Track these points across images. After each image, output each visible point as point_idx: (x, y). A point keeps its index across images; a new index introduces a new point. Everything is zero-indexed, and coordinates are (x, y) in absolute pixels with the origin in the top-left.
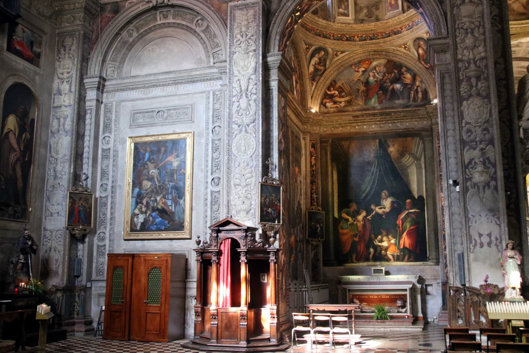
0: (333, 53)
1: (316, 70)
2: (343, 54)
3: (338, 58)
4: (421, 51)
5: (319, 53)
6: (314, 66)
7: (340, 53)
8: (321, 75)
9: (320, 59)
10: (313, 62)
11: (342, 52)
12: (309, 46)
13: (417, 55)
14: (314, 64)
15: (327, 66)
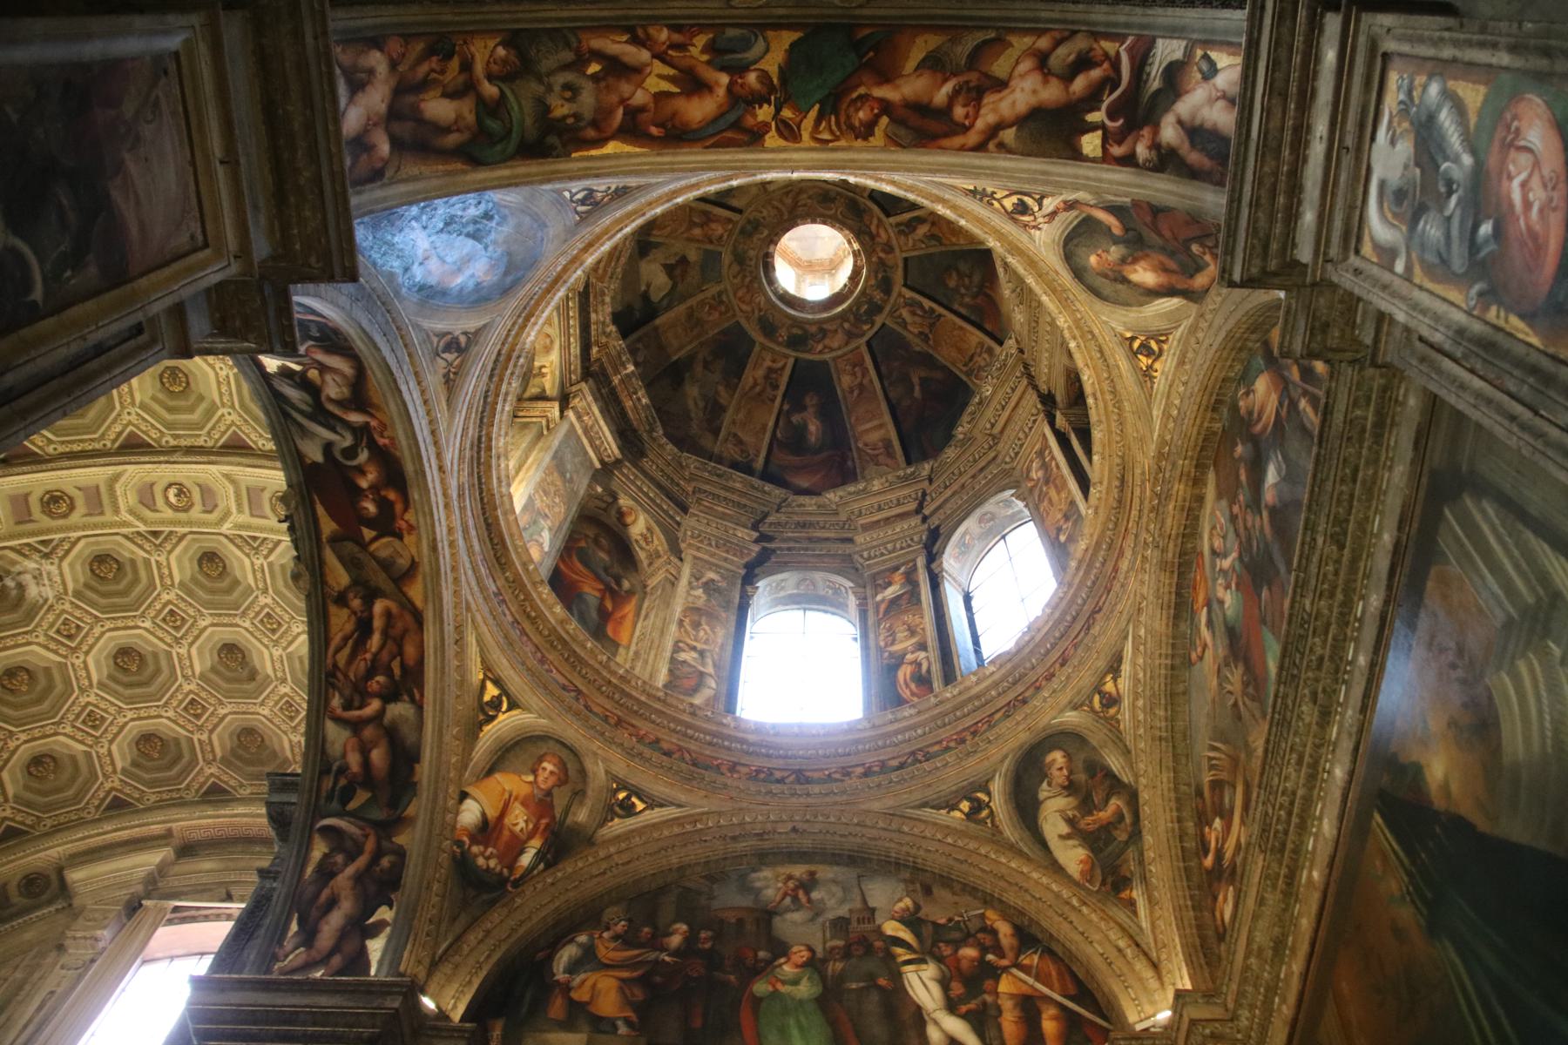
0: (1092, 710)
1: (1096, 840)
2: (1126, 668)
3: (1126, 703)
4: (1144, 275)
5: (1046, 776)
6: (1076, 832)
7: (1115, 679)
8: (1136, 834)
9: (1070, 788)
10: (1053, 825)
11: (1114, 669)
12: (974, 792)
13: (1175, 302)
14: (1064, 829)
15: (1126, 777)
